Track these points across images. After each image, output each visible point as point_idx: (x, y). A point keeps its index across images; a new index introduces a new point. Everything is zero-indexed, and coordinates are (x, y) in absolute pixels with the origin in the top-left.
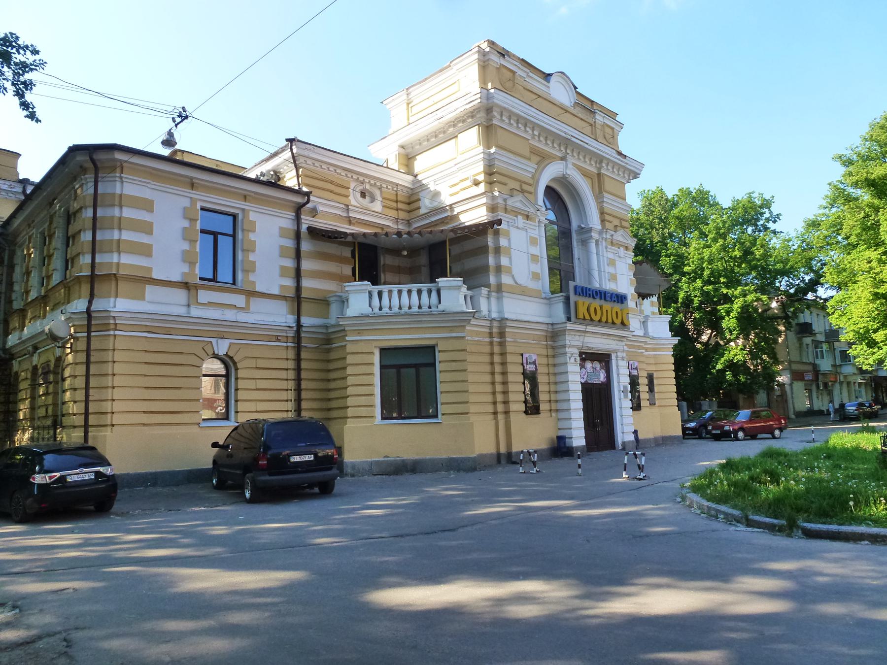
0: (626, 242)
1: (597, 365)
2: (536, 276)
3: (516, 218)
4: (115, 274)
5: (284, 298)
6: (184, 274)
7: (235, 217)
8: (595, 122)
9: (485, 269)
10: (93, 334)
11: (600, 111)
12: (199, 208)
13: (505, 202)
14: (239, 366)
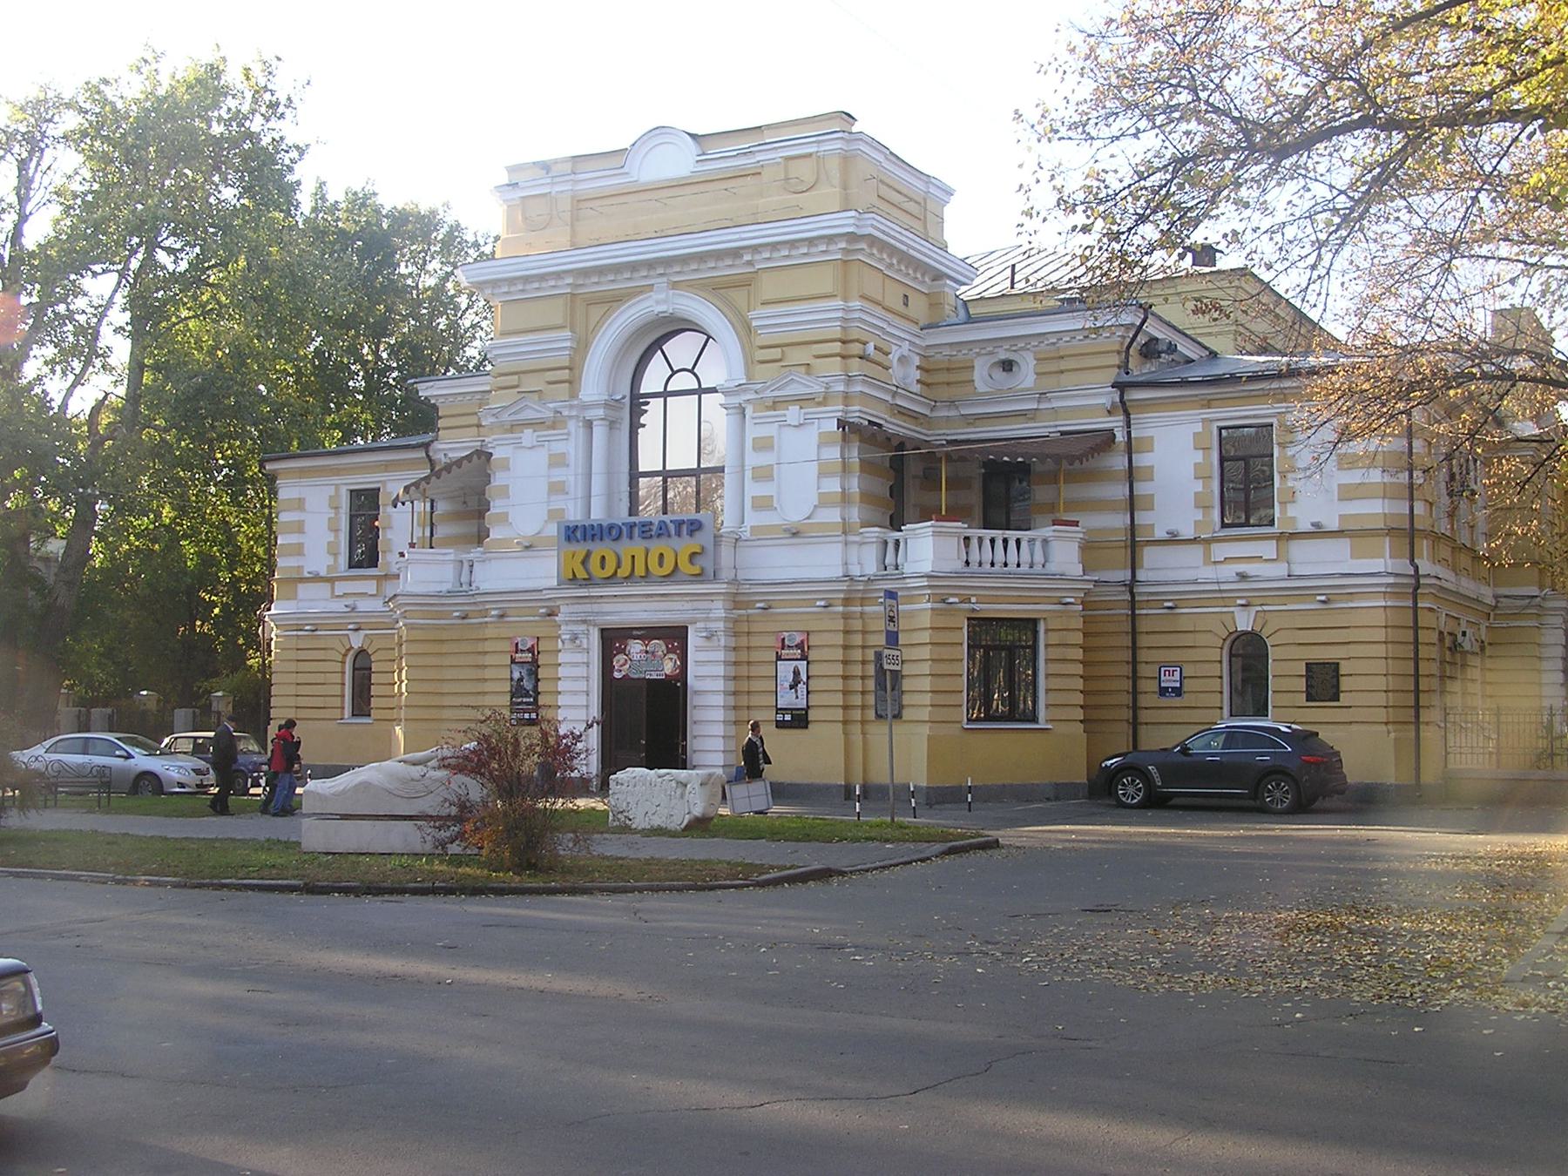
1: (658, 645)
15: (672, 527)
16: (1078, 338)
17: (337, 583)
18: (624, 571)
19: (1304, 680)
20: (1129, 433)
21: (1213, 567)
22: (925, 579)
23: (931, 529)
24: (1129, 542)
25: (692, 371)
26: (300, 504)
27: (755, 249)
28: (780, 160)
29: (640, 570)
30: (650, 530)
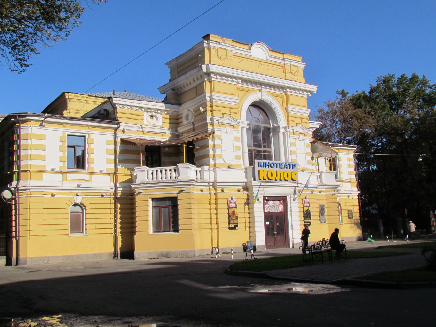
1: (277, 202)
2: (238, 157)
3: (225, 128)
4: (29, 170)
5: (109, 174)
7: (84, 137)
8: (284, 65)
9: (207, 156)
10: (20, 197)
11: (287, 59)
12: (66, 135)
13: (218, 121)
14: (87, 208)
29: (278, 178)
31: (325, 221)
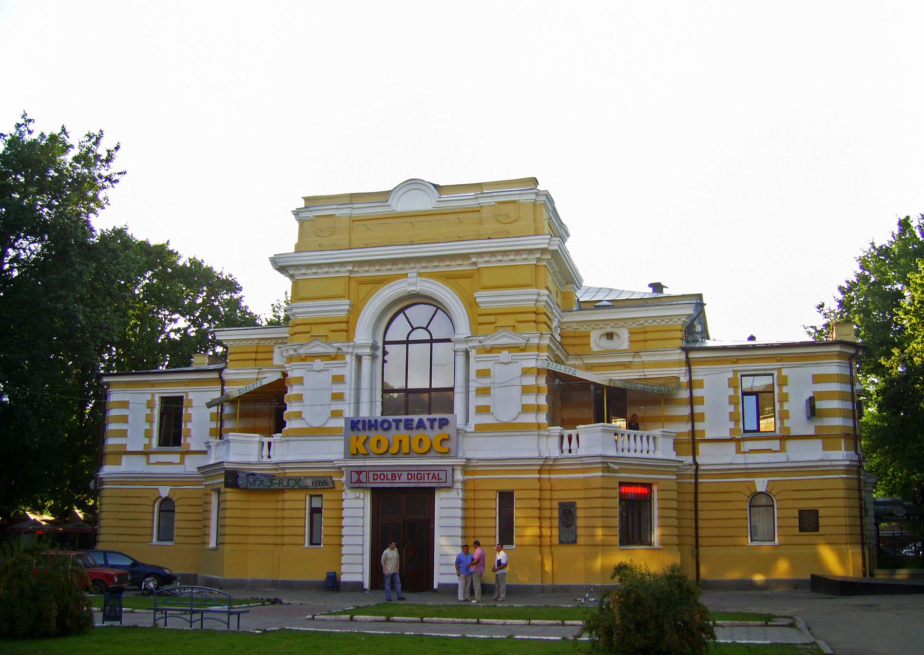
0: (516, 342)
6: (145, 445)
15: (427, 424)
16: (649, 322)
17: (151, 455)
18: (394, 449)
19: (797, 520)
20: (690, 378)
21: (743, 455)
22: (600, 458)
23: (602, 428)
24: (691, 440)
25: (426, 329)
26: (125, 405)
27: (480, 254)
28: (494, 203)
29: (405, 449)
30: (412, 424)
31: (574, 540)
